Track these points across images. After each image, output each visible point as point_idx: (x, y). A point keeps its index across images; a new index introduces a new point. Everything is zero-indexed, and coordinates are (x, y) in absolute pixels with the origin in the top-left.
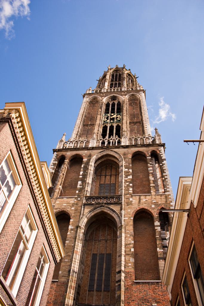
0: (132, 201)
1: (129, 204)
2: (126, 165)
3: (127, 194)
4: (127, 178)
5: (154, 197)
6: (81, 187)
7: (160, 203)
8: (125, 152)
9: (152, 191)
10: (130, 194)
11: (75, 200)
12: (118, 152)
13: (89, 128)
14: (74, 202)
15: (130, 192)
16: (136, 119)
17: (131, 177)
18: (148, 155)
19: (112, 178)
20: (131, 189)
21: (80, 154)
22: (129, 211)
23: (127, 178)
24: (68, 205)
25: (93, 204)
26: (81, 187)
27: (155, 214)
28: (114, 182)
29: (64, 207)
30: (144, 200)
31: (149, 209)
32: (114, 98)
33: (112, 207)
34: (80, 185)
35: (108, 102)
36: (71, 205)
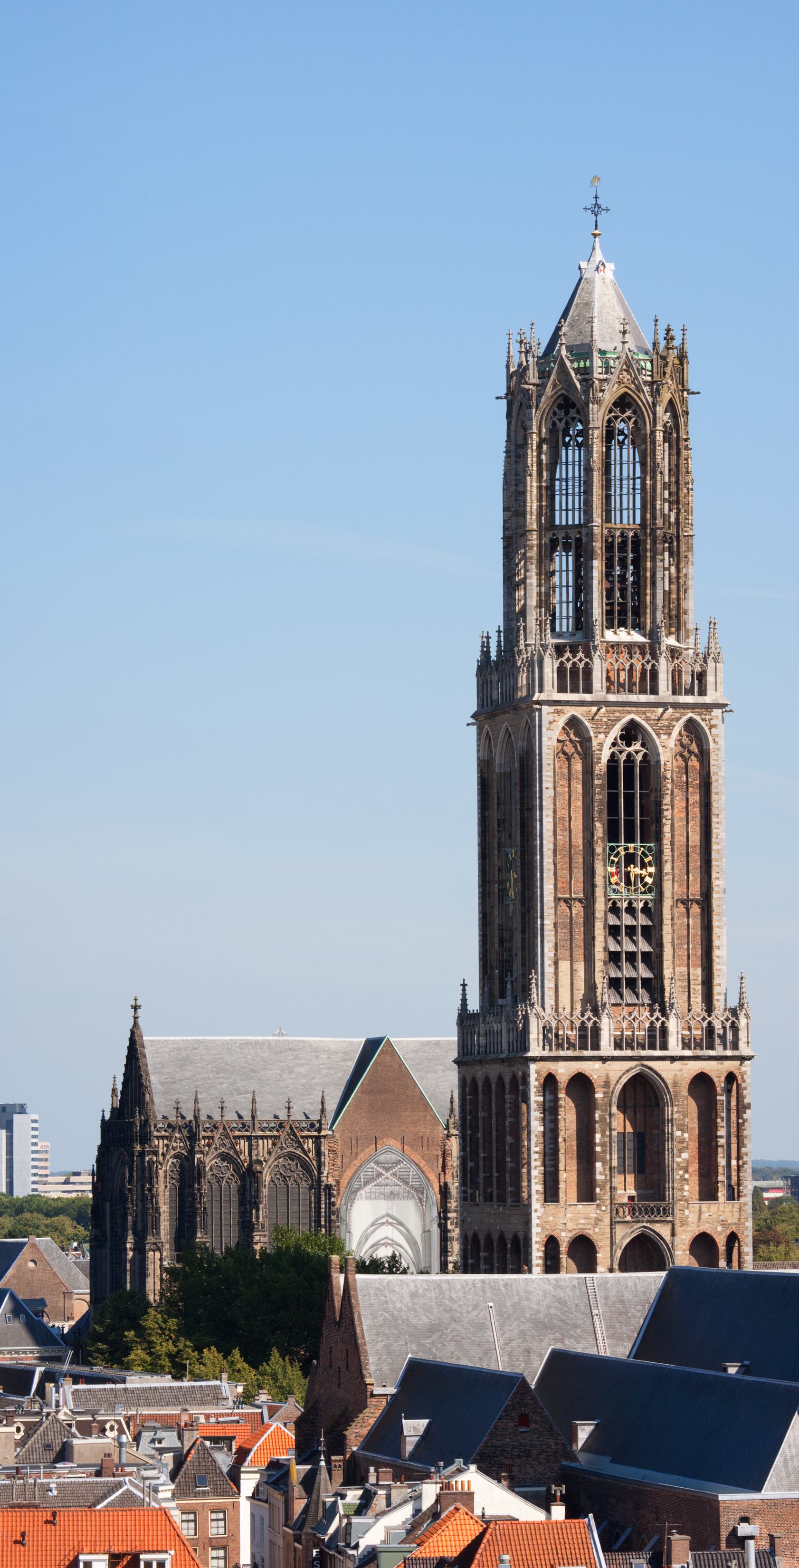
0: (688, 1217)
1: (684, 1223)
2: (679, 1119)
3: (680, 1200)
4: (680, 1156)
5: (721, 1206)
6: (603, 1177)
7: (729, 1222)
8: (675, 1075)
9: (720, 1194)
10: (687, 1200)
11: (598, 1211)
12: (664, 1075)
13: (574, 912)
14: (595, 1215)
15: (685, 1194)
16: (690, 876)
17: (685, 1155)
18: (719, 1090)
19: (638, 1115)
20: (686, 1187)
21: (586, 1073)
22: (684, 1237)
23: (680, 1156)
24: (588, 1221)
25: (628, 1222)
26: (603, 1177)
27: (721, 1242)
28: (642, 1130)
29: (581, 1226)
30: (707, 1215)
31: (712, 1234)
32: (631, 732)
33: (657, 1227)
34: (601, 1174)
35: (613, 755)
36: (593, 1222)
